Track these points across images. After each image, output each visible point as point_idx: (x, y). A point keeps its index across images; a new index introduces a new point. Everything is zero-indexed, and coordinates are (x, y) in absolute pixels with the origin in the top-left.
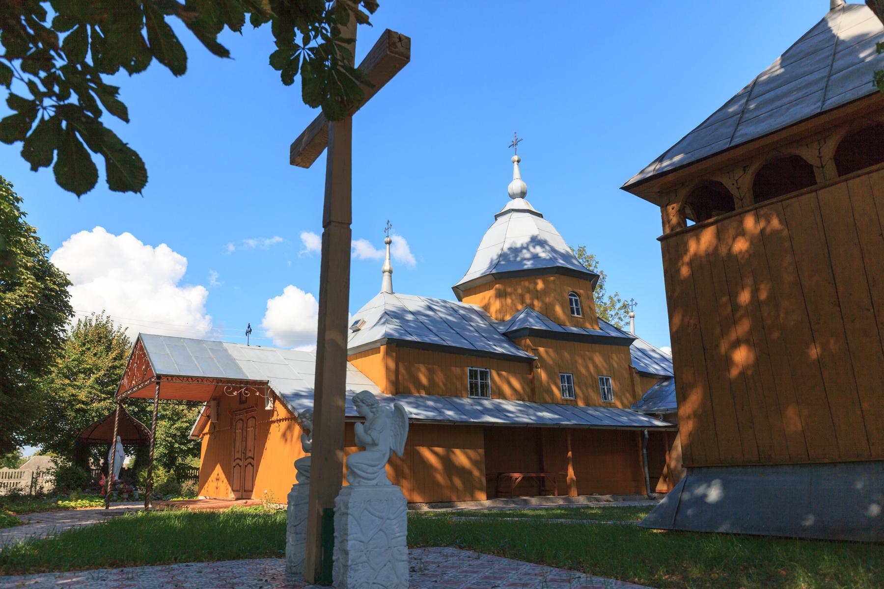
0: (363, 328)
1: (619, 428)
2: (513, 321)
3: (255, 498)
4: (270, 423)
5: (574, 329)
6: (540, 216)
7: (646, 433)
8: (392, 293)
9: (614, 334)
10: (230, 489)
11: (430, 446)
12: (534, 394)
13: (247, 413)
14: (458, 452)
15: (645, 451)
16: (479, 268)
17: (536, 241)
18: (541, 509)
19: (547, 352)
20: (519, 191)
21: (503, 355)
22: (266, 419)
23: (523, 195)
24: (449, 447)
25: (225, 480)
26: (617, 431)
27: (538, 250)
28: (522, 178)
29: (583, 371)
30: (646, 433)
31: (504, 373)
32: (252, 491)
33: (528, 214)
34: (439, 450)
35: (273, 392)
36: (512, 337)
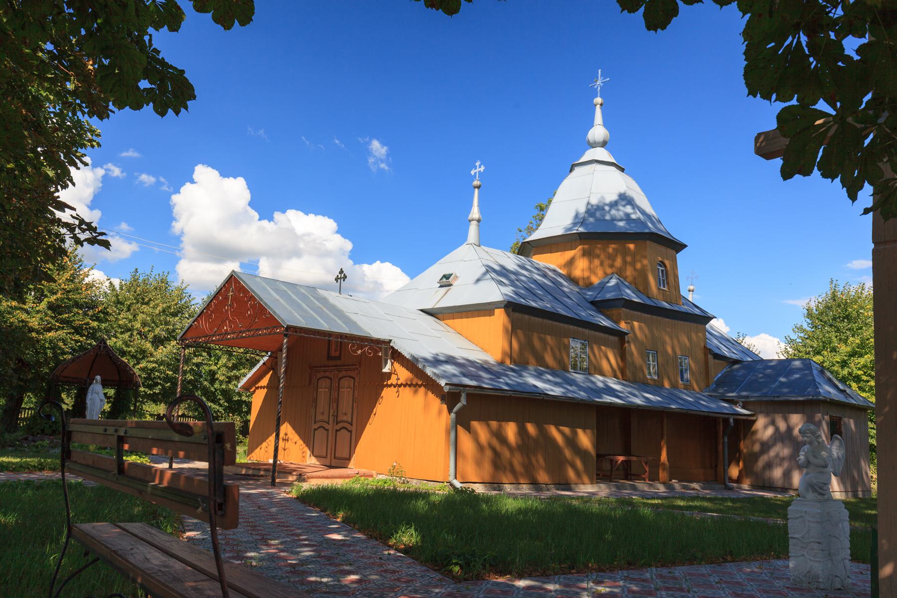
0: (455, 284)
1: (711, 415)
2: (602, 286)
3: (353, 467)
4: (382, 387)
5: (666, 305)
6: (622, 170)
7: (732, 421)
8: (479, 246)
9: (697, 311)
10: (309, 452)
11: (557, 426)
12: (628, 373)
13: (340, 371)
14: (580, 432)
15: (726, 440)
16: (557, 220)
17: (625, 199)
18: (658, 498)
19: (640, 328)
20: (602, 140)
21: (606, 327)
22: (381, 381)
23: (604, 144)
24: (573, 427)
25: (300, 442)
26: (709, 417)
27: (629, 209)
28: (606, 124)
29: (669, 350)
30: (732, 421)
31: (603, 348)
32: (349, 459)
33: (613, 168)
34: (566, 430)
35: (426, 360)
36: (600, 306)
